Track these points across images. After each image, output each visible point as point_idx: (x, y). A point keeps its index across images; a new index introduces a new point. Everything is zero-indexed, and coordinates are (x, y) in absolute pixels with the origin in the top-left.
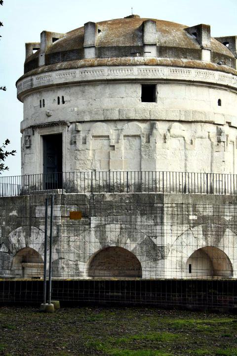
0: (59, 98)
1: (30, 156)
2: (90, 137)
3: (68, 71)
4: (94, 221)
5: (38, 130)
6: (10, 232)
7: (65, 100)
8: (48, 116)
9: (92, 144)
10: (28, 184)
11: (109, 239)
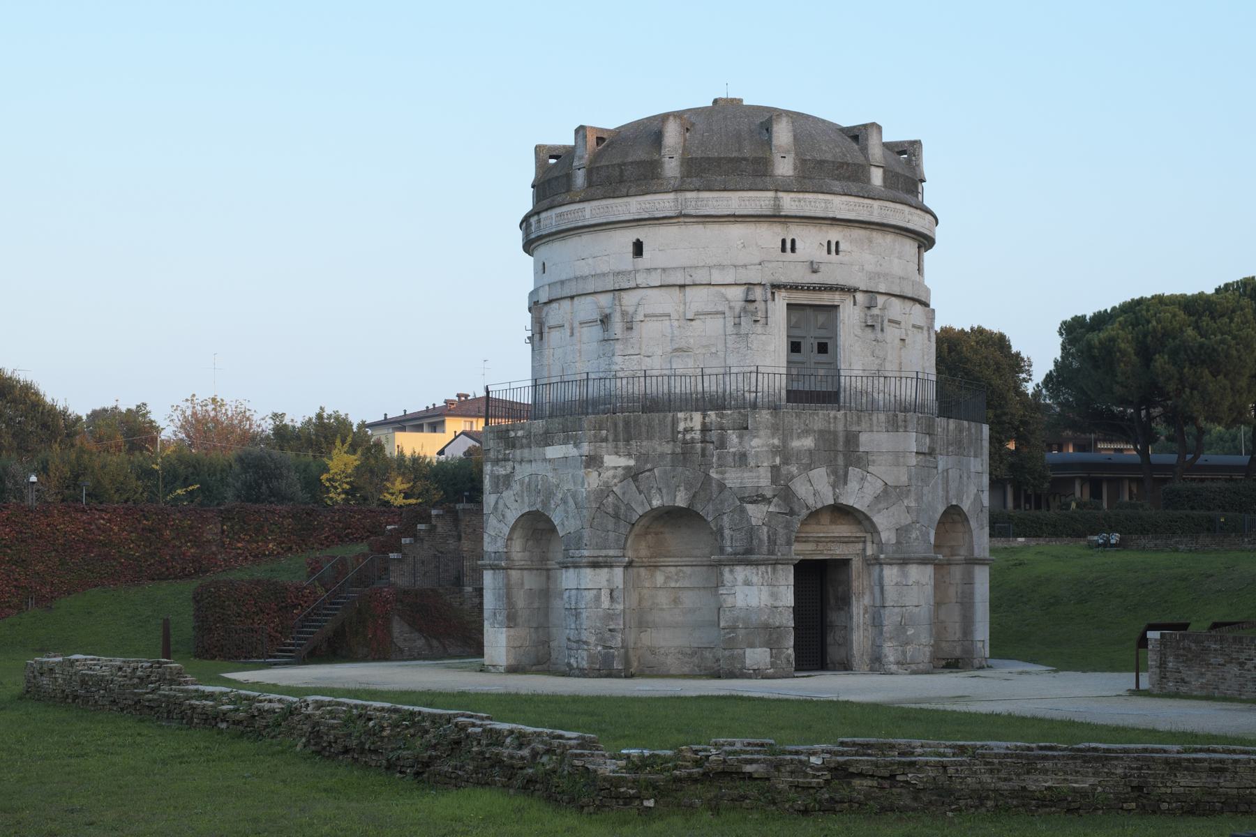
0: (829, 243)
1: (764, 337)
2: (886, 322)
3: (861, 200)
4: (942, 462)
5: (783, 293)
6: (793, 477)
7: (842, 247)
8: (815, 272)
9: (892, 333)
10: (753, 389)
11: (951, 494)
